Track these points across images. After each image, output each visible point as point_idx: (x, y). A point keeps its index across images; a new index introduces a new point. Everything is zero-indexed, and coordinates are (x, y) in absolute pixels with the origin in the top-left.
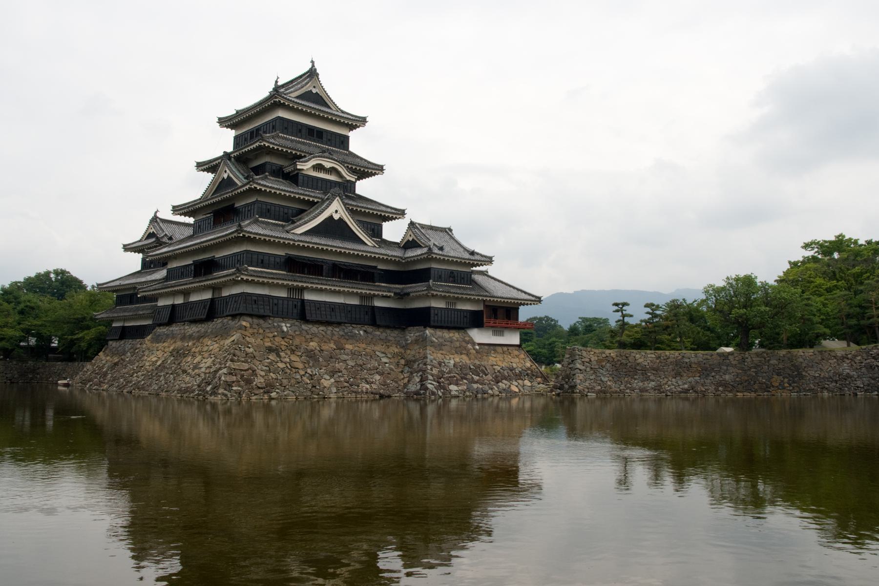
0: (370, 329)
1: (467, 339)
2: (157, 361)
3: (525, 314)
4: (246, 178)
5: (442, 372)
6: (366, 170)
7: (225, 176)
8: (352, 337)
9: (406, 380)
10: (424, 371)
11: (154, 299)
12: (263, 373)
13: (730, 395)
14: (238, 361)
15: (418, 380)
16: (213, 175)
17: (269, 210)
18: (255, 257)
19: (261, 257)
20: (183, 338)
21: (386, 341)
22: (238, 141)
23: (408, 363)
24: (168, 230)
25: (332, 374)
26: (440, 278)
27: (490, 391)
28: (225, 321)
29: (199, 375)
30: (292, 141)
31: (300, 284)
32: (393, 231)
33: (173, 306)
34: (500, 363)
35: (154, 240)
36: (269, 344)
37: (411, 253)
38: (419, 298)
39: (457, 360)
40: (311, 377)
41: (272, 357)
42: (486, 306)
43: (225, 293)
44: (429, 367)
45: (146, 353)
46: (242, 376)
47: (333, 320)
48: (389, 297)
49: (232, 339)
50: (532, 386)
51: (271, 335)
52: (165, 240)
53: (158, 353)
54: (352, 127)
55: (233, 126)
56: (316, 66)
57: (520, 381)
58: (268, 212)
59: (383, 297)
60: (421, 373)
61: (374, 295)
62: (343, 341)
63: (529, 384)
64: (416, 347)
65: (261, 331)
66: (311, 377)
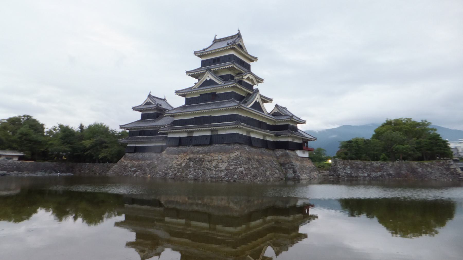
2: (181, 163)
3: (311, 144)
9: (285, 172)
10: (294, 168)
11: (166, 134)
13: (394, 179)
15: (292, 172)
20: (193, 153)
21: (271, 155)
23: (282, 165)
28: (222, 145)
29: (222, 171)
33: (180, 138)
38: (285, 137)
42: (303, 141)
43: (220, 133)
49: (236, 154)
53: (179, 159)
60: (292, 169)
64: (284, 158)
66: (263, 171)
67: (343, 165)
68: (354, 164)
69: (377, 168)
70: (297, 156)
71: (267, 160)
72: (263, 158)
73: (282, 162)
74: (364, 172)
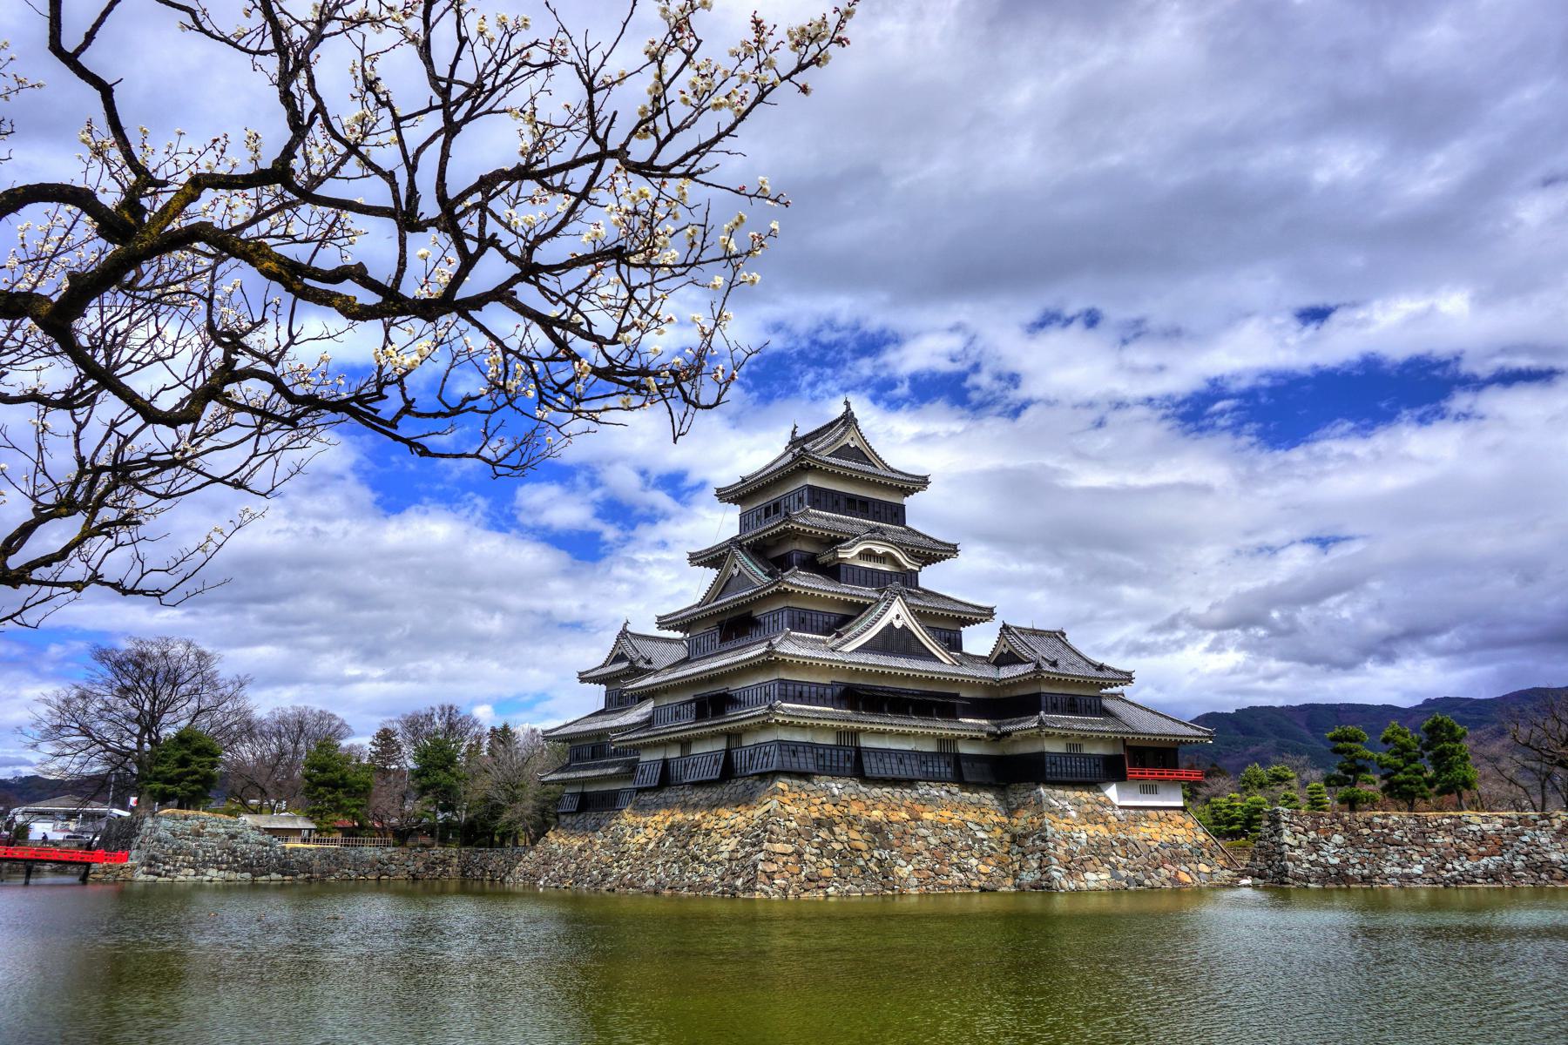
0: (955, 789)
1: (1102, 799)
4: (769, 575)
5: (1069, 852)
6: (934, 552)
7: (736, 572)
8: (932, 801)
9: (1017, 866)
12: (814, 859)
14: (778, 841)
16: (714, 573)
17: (803, 620)
18: (790, 688)
19: (798, 688)
20: (685, 807)
21: (979, 806)
22: (744, 523)
23: (1015, 839)
24: (647, 649)
25: (909, 857)
26: (1054, 709)
27: (1147, 882)
30: (828, 519)
31: (856, 726)
32: (979, 640)
33: (666, 762)
34: (1156, 837)
35: (626, 664)
36: (817, 815)
37: (1006, 673)
38: (1027, 738)
39: (1091, 833)
40: (880, 862)
41: (824, 834)
42: (1128, 748)
44: (1051, 845)
45: (629, 831)
46: (785, 864)
47: (903, 775)
48: (977, 739)
49: (766, 808)
50: (1212, 873)
51: (818, 801)
52: (641, 664)
54: (907, 492)
55: (736, 501)
56: (853, 408)
57: (1192, 865)
58: (802, 622)
59: (972, 738)
61: (959, 737)
62: (919, 808)
63: (1206, 869)
65: (804, 796)
66: (880, 862)
67: (1312, 834)
68: (1368, 824)
69: (1483, 838)
70: (1108, 803)
71: (935, 826)
72: (919, 819)
73: (1019, 830)
74: (1410, 859)
